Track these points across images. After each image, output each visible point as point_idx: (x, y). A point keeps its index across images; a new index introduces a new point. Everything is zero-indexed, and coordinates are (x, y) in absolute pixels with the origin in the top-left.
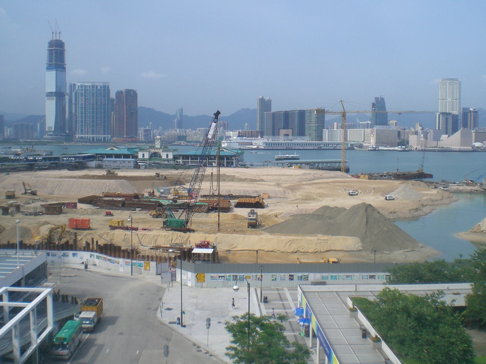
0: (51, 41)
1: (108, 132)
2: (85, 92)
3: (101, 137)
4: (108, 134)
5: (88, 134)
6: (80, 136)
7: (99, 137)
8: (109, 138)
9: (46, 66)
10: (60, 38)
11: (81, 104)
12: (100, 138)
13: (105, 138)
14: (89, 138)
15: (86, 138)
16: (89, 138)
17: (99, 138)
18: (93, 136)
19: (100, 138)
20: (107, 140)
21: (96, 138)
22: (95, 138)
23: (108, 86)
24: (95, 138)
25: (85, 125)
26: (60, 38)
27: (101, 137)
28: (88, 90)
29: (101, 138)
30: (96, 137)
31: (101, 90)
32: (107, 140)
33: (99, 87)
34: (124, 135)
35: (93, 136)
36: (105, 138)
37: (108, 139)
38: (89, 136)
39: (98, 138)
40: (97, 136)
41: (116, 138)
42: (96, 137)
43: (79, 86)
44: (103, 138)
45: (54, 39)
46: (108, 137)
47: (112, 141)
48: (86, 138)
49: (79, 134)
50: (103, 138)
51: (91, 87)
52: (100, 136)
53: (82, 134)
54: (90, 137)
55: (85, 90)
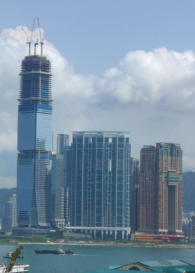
0: (27, 58)
1: (126, 221)
3: (113, 231)
4: (126, 226)
7: (109, 231)
8: (129, 232)
9: (18, 104)
10: (42, 53)
11: (78, 172)
12: (111, 233)
13: (120, 233)
14: (91, 232)
15: (86, 232)
16: (91, 232)
19: (111, 233)
20: (123, 238)
21: (105, 233)
22: (102, 233)
23: (128, 139)
24: (102, 233)
25: (85, 209)
26: (42, 53)
28: (90, 147)
29: (114, 233)
32: (123, 238)
33: (110, 141)
36: (120, 233)
37: (125, 235)
39: (107, 233)
41: (141, 234)
42: (105, 231)
44: (116, 233)
45: (32, 54)
46: (125, 232)
47: (132, 238)
48: (86, 232)
50: (116, 233)
52: (111, 228)
53: (79, 225)
54: (93, 230)
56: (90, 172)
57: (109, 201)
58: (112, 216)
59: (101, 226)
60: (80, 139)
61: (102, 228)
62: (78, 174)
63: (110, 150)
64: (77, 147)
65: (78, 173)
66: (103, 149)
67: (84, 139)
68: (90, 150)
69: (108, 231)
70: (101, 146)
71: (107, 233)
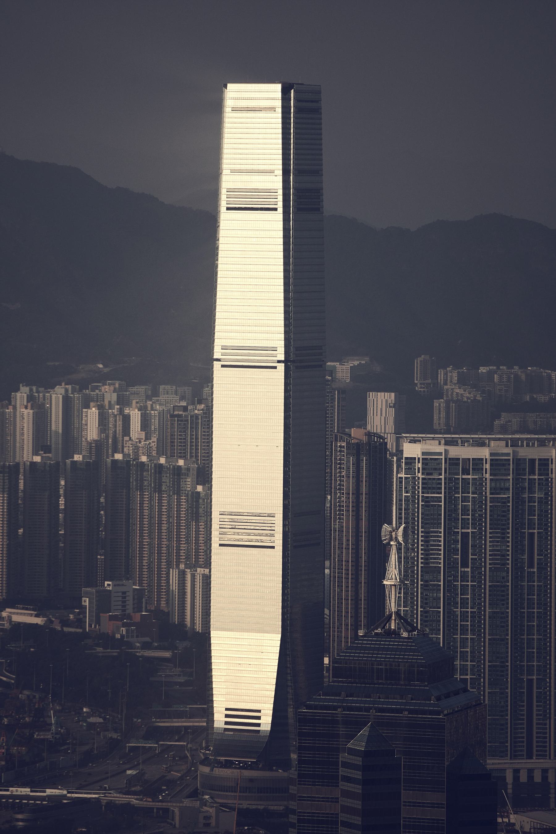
2: (450, 500)
3: (545, 771)
7: (530, 771)
12: (538, 778)
19: (538, 778)
21: (516, 778)
22: (509, 778)
24: (509, 778)
27: (545, 771)
29: (545, 778)
30: (516, 771)
39: (523, 778)
40: (523, 764)
43: (410, 461)
51: (488, 466)
52: (537, 763)
55: (452, 487)
58: (539, 719)
59: (507, 756)
62: (427, 581)
64: (423, 488)
65: (427, 577)
66: (509, 497)
67: (445, 462)
69: (528, 770)
70: (502, 489)
71: (523, 778)
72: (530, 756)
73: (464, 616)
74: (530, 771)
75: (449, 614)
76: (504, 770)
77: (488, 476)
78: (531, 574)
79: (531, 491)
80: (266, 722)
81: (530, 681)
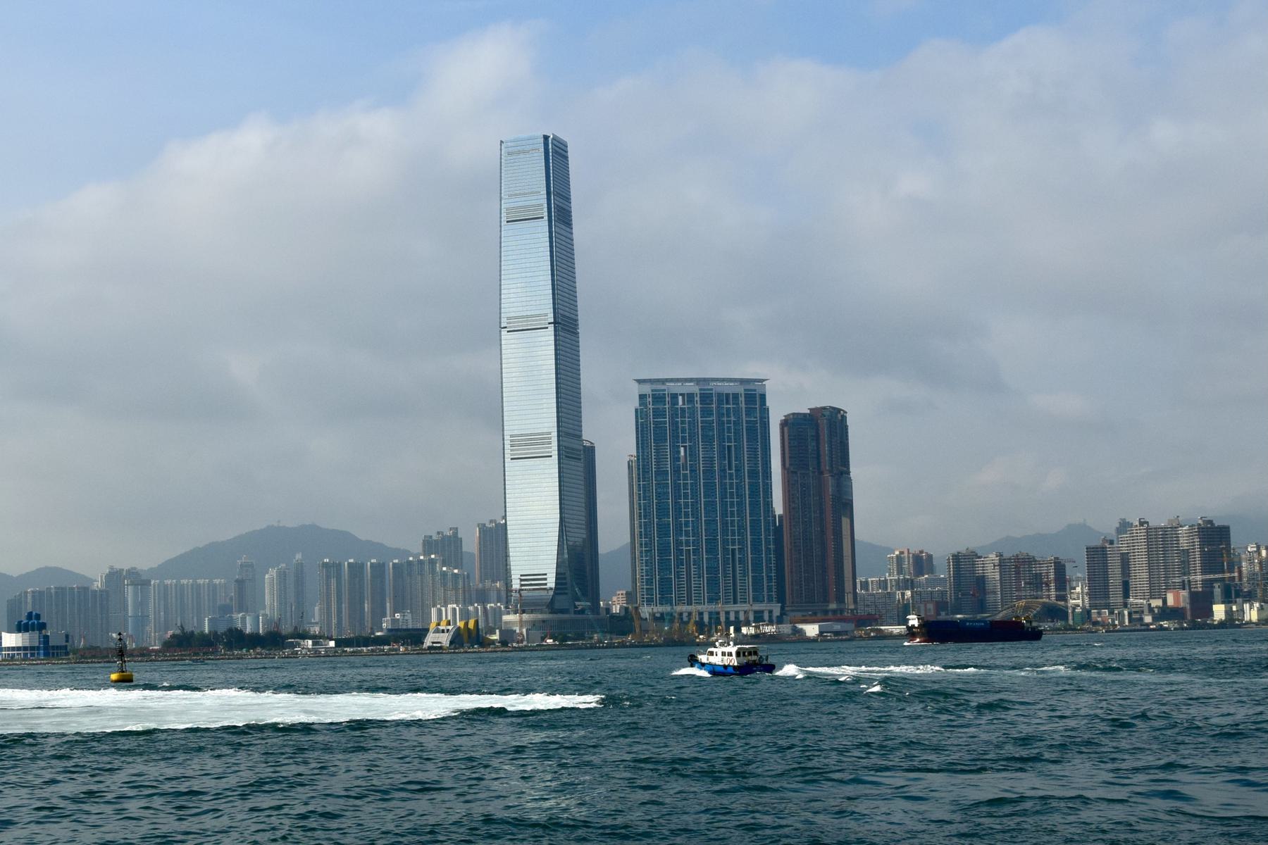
1: (770, 589)
4: (770, 600)
5: (690, 603)
6: (659, 609)
7: (737, 613)
8: (777, 612)
17: (737, 618)
18: (712, 607)
21: (727, 618)
23: (763, 397)
28: (683, 416)
30: (727, 613)
31: (737, 411)
34: (826, 601)
35: (712, 607)
38: (693, 608)
39: (732, 618)
40: (732, 608)
46: (771, 612)
49: (650, 601)
53: (665, 600)
56: (685, 475)
57: (733, 544)
60: (658, 398)
61: (719, 607)
63: (729, 422)
68: (683, 422)
71: (732, 618)
72: (735, 602)
73: (686, 505)
74: (737, 613)
75: (676, 503)
76: (718, 613)
77: (699, 405)
78: (731, 475)
79: (728, 416)
80: (551, 582)
81: (733, 550)
